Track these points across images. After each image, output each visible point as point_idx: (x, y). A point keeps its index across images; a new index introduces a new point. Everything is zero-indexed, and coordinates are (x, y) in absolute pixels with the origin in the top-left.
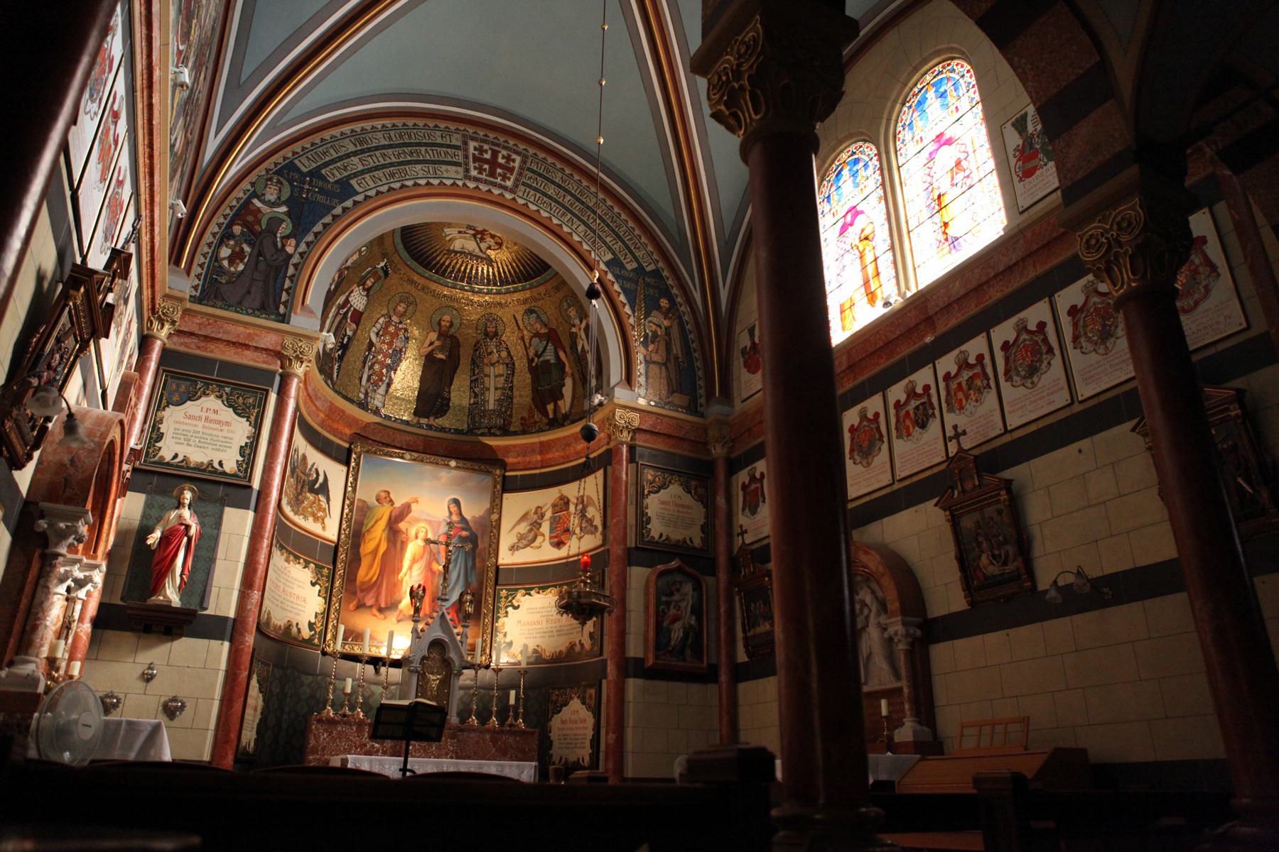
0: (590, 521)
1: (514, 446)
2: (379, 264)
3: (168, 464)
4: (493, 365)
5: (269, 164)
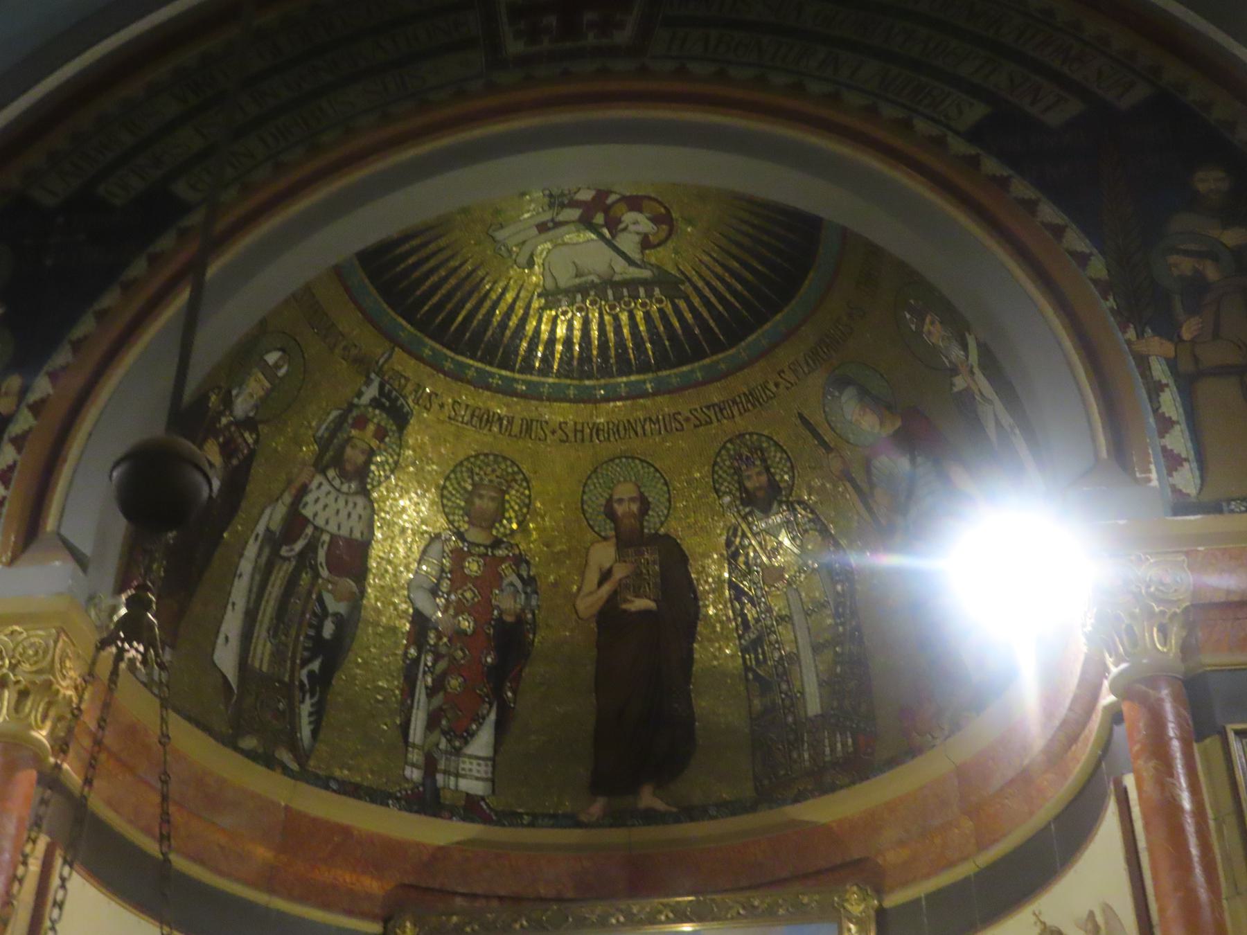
2: (360, 394)
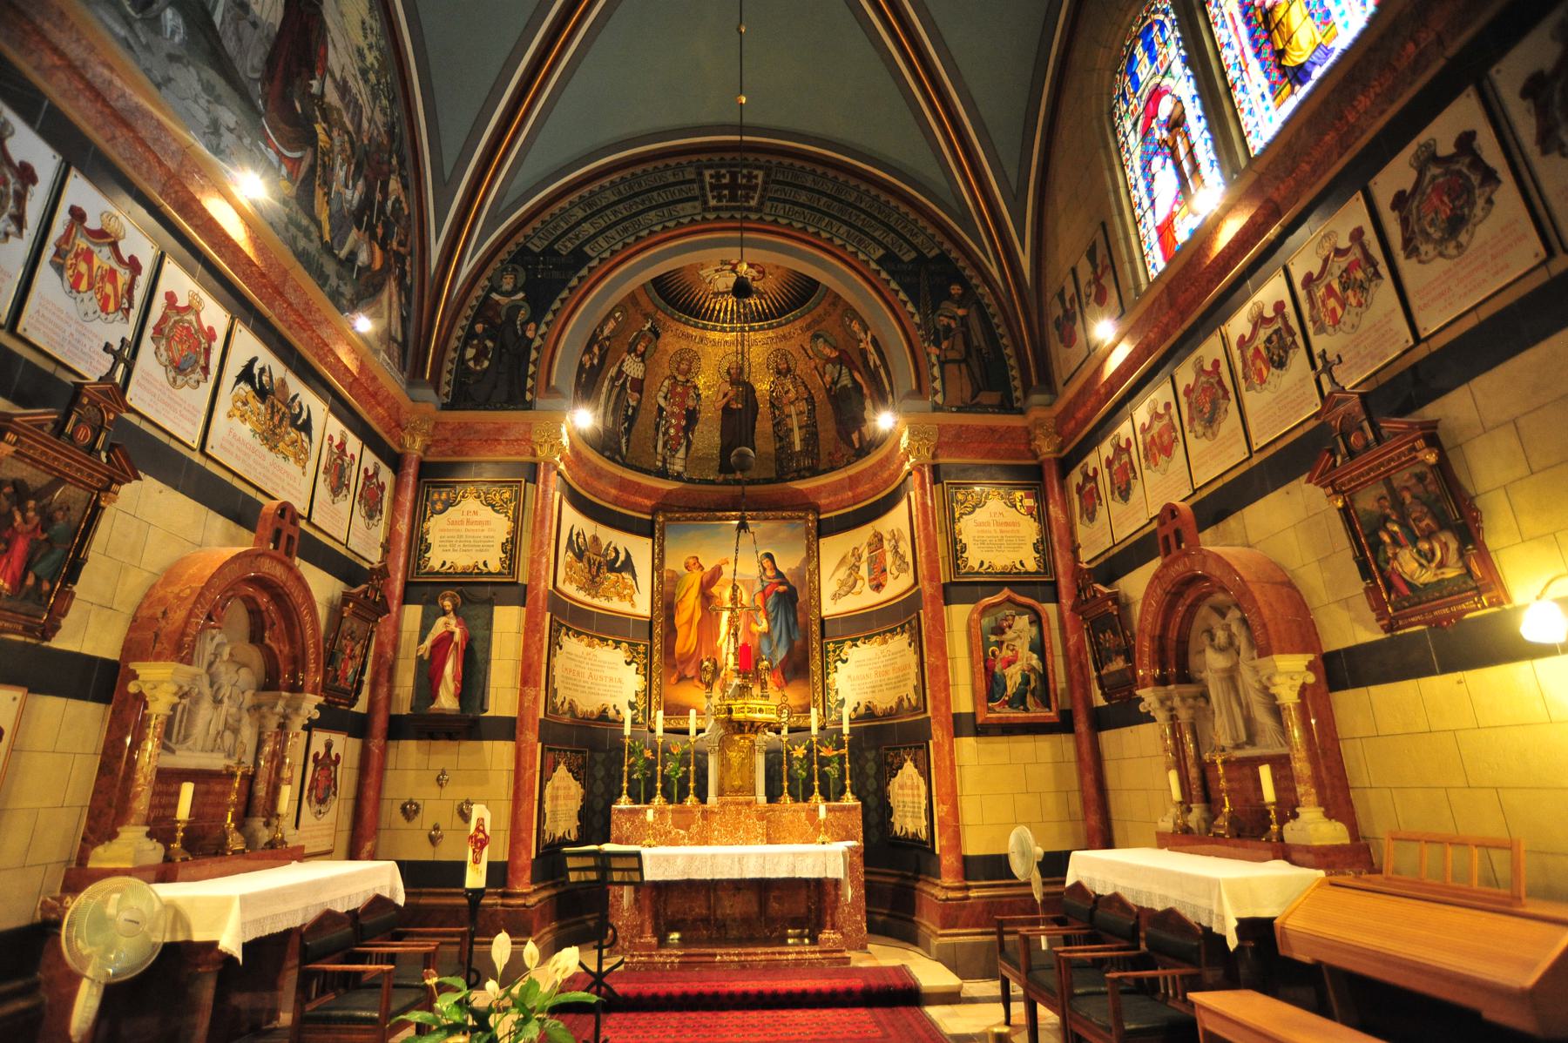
0: (902, 557)
1: (824, 486)
3: (438, 573)
4: (792, 403)
5: (503, 255)
